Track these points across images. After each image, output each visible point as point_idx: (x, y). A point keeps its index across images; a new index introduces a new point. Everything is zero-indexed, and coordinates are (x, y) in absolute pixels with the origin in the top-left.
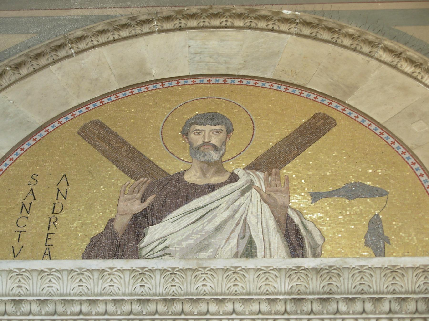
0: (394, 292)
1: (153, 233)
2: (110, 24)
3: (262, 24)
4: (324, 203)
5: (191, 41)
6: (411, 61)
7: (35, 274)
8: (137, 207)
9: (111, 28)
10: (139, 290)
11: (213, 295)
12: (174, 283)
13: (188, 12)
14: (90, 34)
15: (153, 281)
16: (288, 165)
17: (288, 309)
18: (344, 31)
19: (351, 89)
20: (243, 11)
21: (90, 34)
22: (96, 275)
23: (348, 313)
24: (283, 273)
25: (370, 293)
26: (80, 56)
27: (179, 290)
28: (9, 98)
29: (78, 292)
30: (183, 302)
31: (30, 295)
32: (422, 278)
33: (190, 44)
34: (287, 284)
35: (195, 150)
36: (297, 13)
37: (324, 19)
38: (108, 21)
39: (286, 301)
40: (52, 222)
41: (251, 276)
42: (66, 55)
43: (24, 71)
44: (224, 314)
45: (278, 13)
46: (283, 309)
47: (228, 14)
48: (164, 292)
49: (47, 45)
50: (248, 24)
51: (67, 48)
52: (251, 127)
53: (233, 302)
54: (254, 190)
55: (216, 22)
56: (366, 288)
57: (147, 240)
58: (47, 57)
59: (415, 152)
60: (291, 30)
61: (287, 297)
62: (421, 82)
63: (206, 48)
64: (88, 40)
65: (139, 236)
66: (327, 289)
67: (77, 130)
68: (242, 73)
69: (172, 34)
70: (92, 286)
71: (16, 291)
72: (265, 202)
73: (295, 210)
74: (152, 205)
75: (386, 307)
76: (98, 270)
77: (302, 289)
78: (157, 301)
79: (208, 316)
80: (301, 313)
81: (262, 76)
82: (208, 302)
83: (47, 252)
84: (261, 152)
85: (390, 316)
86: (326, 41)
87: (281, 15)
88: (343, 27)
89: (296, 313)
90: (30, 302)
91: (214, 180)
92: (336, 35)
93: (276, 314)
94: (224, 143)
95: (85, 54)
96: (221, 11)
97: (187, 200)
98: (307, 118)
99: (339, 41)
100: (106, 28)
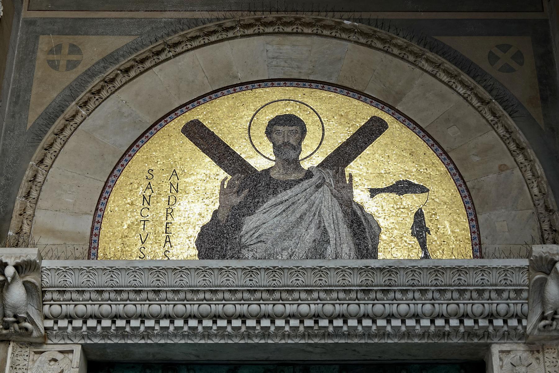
0: (436, 285)
1: (250, 223)
2: (201, 30)
3: (326, 32)
5: (268, 46)
6: (447, 72)
7: (170, 271)
8: (236, 200)
9: (202, 34)
10: (249, 283)
11: (304, 286)
12: (274, 278)
13: (265, 20)
14: (185, 39)
15: (259, 276)
16: (351, 164)
17: (359, 297)
18: (394, 41)
19: (400, 96)
20: (311, 21)
21: (185, 39)
22: (216, 272)
23: (402, 300)
24: (356, 271)
25: (419, 286)
26: (177, 58)
27: (278, 283)
28: (122, 98)
29: (203, 284)
30: (281, 291)
31: (167, 287)
32: (457, 275)
33: (268, 49)
34: (358, 279)
35: (277, 149)
36: (355, 23)
37: (378, 30)
38: (199, 27)
39: (357, 291)
40: (169, 213)
41: (332, 273)
42: (165, 58)
43: (132, 74)
44: (311, 300)
45: (340, 23)
46: (355, 297)
47: (298, 22)
48: (268, 284)
49: (150, 50)
50: (315, 31)
51: (166, 52)
52: (321, 128)
53: (319, 291)
54: (325, 186)
55: (289, 29)
56: (416, 282)
57: (245, 228)
58: (150, 61)
59: (450, 155)
60: (351, 38)
61: (358, 288)
62: (455, 90)
63: (281, 53)
64: (183, 45)
65: (238, 227)
66: (387, 283)
67: (181, 128)
68: (311, 78)
69: (252, 38)
70: (213, 280)
72: (335, 197)
73: (358, 204)
74: (246, 197)
75: (430, 295)
76: (218, 268)
77: (370, 282)
78: (262, 291)
79: (300, 302)
80: (368, 300)
81: (328, 81)
82: (299, 291)
83: (168, 240)
84: (329, 152)
85: (433, 302)
86: (379, 49)
87: (343, 25)
88: (393, 38)
89: (364, 300)
90: (166, 292)
91: (293, 177)
92: (387, 45)
93: (349, 300)
94: (300, 144)
95: (181, 56)
96: (293, 19)
97: (275, 193)
98: (366, 121)
99: (390, 50)
100: (198, 34)
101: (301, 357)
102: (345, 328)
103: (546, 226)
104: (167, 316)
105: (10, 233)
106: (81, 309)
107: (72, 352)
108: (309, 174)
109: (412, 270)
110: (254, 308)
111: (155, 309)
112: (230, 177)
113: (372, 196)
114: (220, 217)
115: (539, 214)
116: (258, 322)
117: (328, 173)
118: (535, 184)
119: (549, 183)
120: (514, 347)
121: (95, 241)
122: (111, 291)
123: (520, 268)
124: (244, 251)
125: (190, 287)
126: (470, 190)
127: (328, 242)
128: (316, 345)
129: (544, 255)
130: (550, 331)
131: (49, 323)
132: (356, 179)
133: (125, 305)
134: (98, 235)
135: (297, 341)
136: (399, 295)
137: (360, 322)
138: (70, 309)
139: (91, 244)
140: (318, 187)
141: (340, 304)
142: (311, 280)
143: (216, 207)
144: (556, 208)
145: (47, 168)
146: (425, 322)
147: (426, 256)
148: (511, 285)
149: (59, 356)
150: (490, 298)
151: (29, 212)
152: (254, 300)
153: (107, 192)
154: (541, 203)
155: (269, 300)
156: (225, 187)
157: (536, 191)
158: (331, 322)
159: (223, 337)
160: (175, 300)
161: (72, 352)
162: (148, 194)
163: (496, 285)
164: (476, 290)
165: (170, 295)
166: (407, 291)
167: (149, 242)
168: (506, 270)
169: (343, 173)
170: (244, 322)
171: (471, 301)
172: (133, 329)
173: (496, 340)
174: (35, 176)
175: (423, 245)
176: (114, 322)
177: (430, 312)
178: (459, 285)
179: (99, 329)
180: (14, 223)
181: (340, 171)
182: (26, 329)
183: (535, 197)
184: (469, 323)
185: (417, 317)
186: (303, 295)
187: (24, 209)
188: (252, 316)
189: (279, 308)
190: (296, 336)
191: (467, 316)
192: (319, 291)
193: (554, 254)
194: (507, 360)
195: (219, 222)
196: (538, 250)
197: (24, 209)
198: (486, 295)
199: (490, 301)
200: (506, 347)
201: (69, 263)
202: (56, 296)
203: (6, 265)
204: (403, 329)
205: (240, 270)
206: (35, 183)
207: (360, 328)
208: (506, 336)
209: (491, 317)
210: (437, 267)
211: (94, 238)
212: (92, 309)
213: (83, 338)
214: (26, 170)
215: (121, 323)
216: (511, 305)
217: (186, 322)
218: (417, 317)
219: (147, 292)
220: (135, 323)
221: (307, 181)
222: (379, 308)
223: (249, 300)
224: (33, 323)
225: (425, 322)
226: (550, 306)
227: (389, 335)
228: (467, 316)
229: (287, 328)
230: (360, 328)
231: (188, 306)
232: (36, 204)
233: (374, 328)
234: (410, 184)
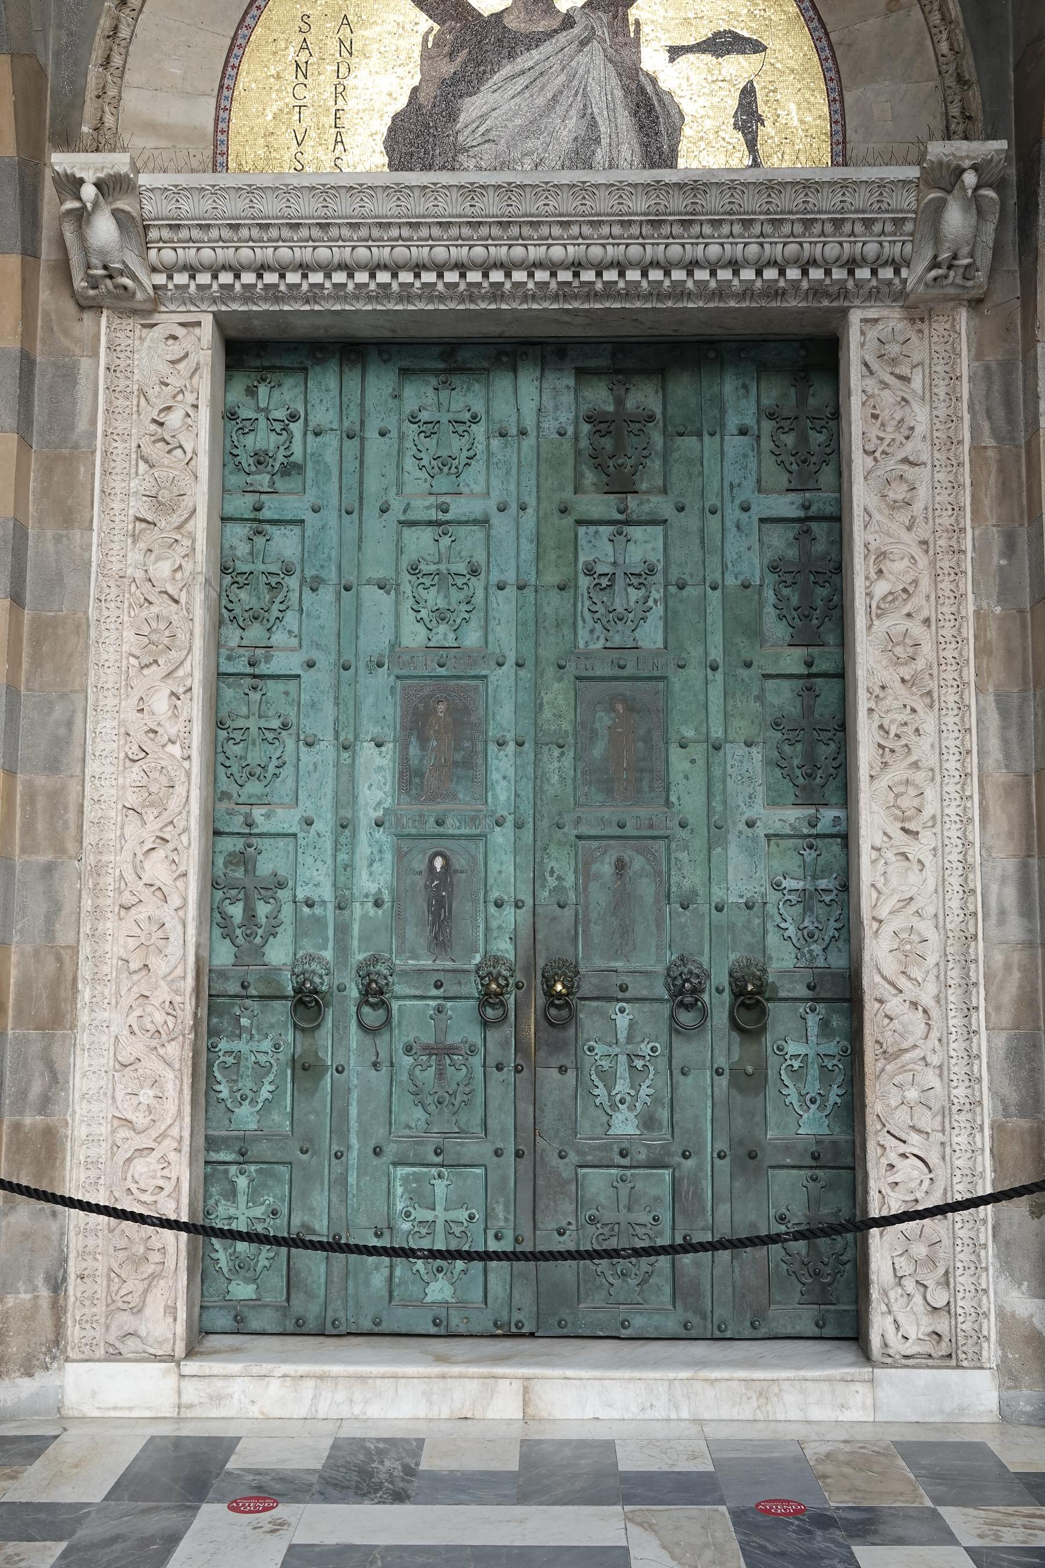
1: (471, 108)
4: (686, 61)
7: (344, 191)
8: (447, 69)
10: (469, 211)
22: (417, 192)
23: (713, 237)
24: (640, 189)
30: (520, 224)
39: (641, 222)
40: (340, 92)
41: (602, 193)
53: (580, 224)
56: (736, 208)
57: (463, 118)
65: (452, 116)
66: (690, 209)
71: (322, 212)
72: (611, 61)
74: (465, 63)
75: (757, 229)
77: (661, 208)
78: (490, 224)
79: (550, 241)
80: (659, 237)
82: (550, 224)
85: (761, 240)
89: (653, 237)
90: (339, 226)
91: (543, 26)
93: (629, 238)
97: (511, 56)
101: (553, 331)
102: (621, 285)
103: (955, 110)
104: (342, 266)
105: (85, 129)
106: (207, 254)
107: (198, 324)
108: (568, 21)
109: (729, 185)
110: (479, 252)
111: (323, 254)
112: (437, 27)
113: (672, 60)
114: (422, 98)
115: (945, 88)
116: (486, 275)
117: (600, 18)
118: (945, 36)
119: (968, 33)
120: (886, 312)
121: (222, 142)
122: (252, 225)
123: (905, 182)
124: (462, 158)
125: (376, 217)
126: (835, 47)
127: (598, 141)
128: (575, 312)
129: (945, 159)
130: (942, 287)
131: (160, 279)
132: (645, 29)
133: (276, 248)
134: (226, 132)
135: (546, 305)
136: (707, 230)
137: (645, 274)
138: (190, 255)
139: (216, 146)
140: (583, 43)
141: (613, 245)
142: (567, 204)
143: (416, 82)
144: (974, 79)
145: (134, 14)
146: (748, 274)
147: (756, 164)
148: (887, 211)
149: (180, 332)
150: (853, 234)
151: (112, 92)
152: (478, 239)
153: (236, 56)
154: (952, 68)
155: (501, 238)
156: (430, 45)
157: (944, 47)
158: (599, 274)
159: (431, 299)
160: (353, 240)
161: (198, 324)
162: (304, 60)
163: (864, 212)
164: (832, 219)
165: (346, 232)
166: (720, 221)
167: (308, 143)
168: (881, 185)
169: (625, 19)
170: (463, 275)
171: (822, 239)
172: (290, 286)
173: (857, 302)
174: (116, 28)
175: (752, 145)
176: (260, 276)
177: (756, 257)
178: (806, 211)
179: (238, 287)
180: (89, 109)
181: (620, 14)
182: (125, 288)
183: (941, 59)
184: (817, 274)
185: (735, 266)
186: (556, 231)
187: (104, 87)
188: (475, 266)
189: (518, 252)
190: (545, 298)
191: (813, 262)
192: (580, 224)
193: (961, 158)
194: (872, 334)
195: (420, 107)
196: (938, 150)
197: (104, 87)
198: (847, 228)
199: (852, 239)
200: (872, 314)
201: (183, 179)
202: (166, 234)
203: (81, 181)
204: (713, 284)
205: (455, 189)
206: (117, 41)
207: (644, 284)
208: (874, 295)
209: (851, 265)
210: (770, 181)
211: (220, 137)
212: (226, 255)
213: (215, 302)
214: (99, 19)
215: (271, 278)
216: (886, 244)
217: (373, 276)
218: (735, 266)
219: (309, 226)
220: (293, 278)
221: (564, 33)
222: (675, 251)
223: (471, 238)
224: (134, 277)
225: (748, 274)
226: (948, 245)
227: (690, 295)
228: (813, 262)
229: (531, 285)
230: (644, 284)
231: (374, 250)
232: (121, 78)
233: (667, 283)
234: (737, 38)
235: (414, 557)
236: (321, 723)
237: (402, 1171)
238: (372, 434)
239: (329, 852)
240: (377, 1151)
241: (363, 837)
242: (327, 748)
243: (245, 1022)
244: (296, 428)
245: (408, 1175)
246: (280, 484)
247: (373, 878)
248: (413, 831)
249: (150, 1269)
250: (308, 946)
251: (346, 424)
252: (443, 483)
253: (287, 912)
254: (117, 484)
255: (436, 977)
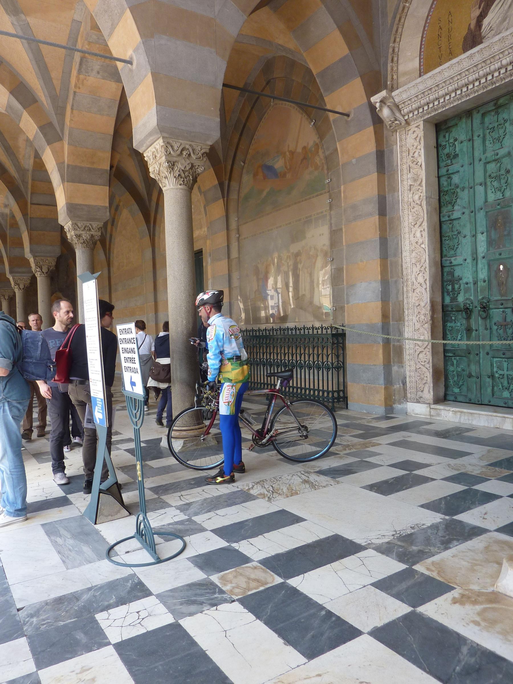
106: (414, 106)
202: (403, 105)
235: (490, 172)
236: (467, 231)
237: (495, 360)
238: (475, 138)
239: (471, 268)
240: (488, 354)
241: (479, 262)
242: (468, 237)
243: (453, 318)
244: (456, 143)
245: (497, 361)
246: (454, 161)
247: (483, 274)
248: (493, 258)
249: (425, 382)
250: (467, 296)
251: (468, 137)
252: (498, 145)
253: (462, 287)
254: (405, 177)
255: (501, 302)
